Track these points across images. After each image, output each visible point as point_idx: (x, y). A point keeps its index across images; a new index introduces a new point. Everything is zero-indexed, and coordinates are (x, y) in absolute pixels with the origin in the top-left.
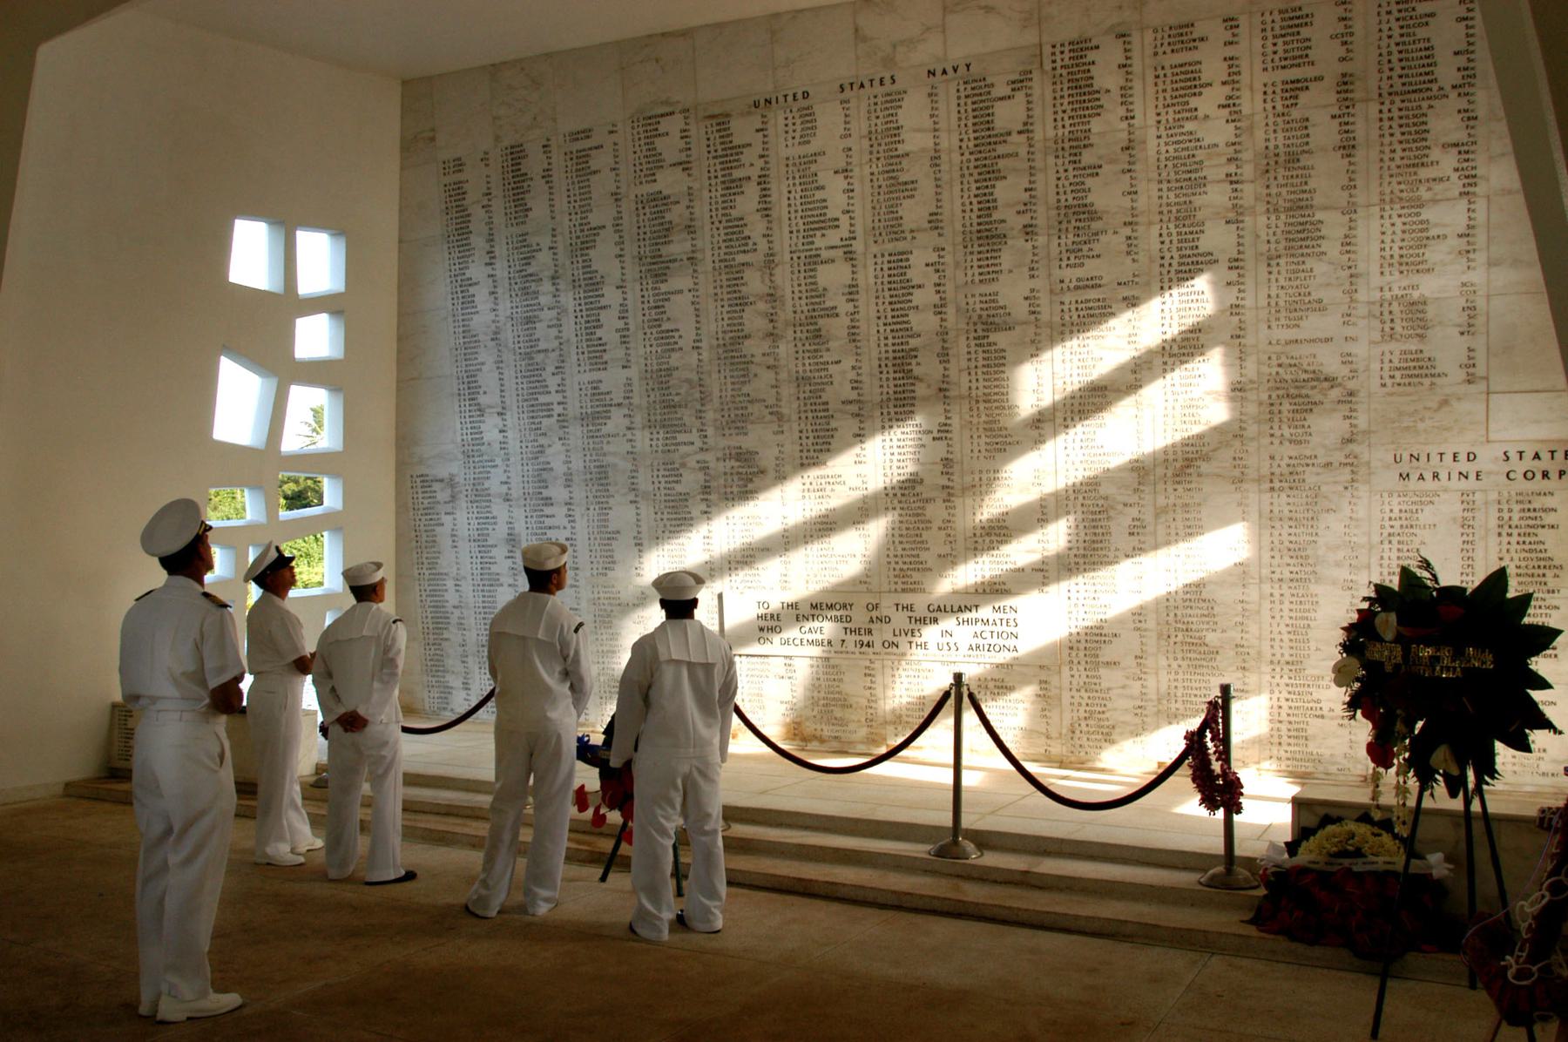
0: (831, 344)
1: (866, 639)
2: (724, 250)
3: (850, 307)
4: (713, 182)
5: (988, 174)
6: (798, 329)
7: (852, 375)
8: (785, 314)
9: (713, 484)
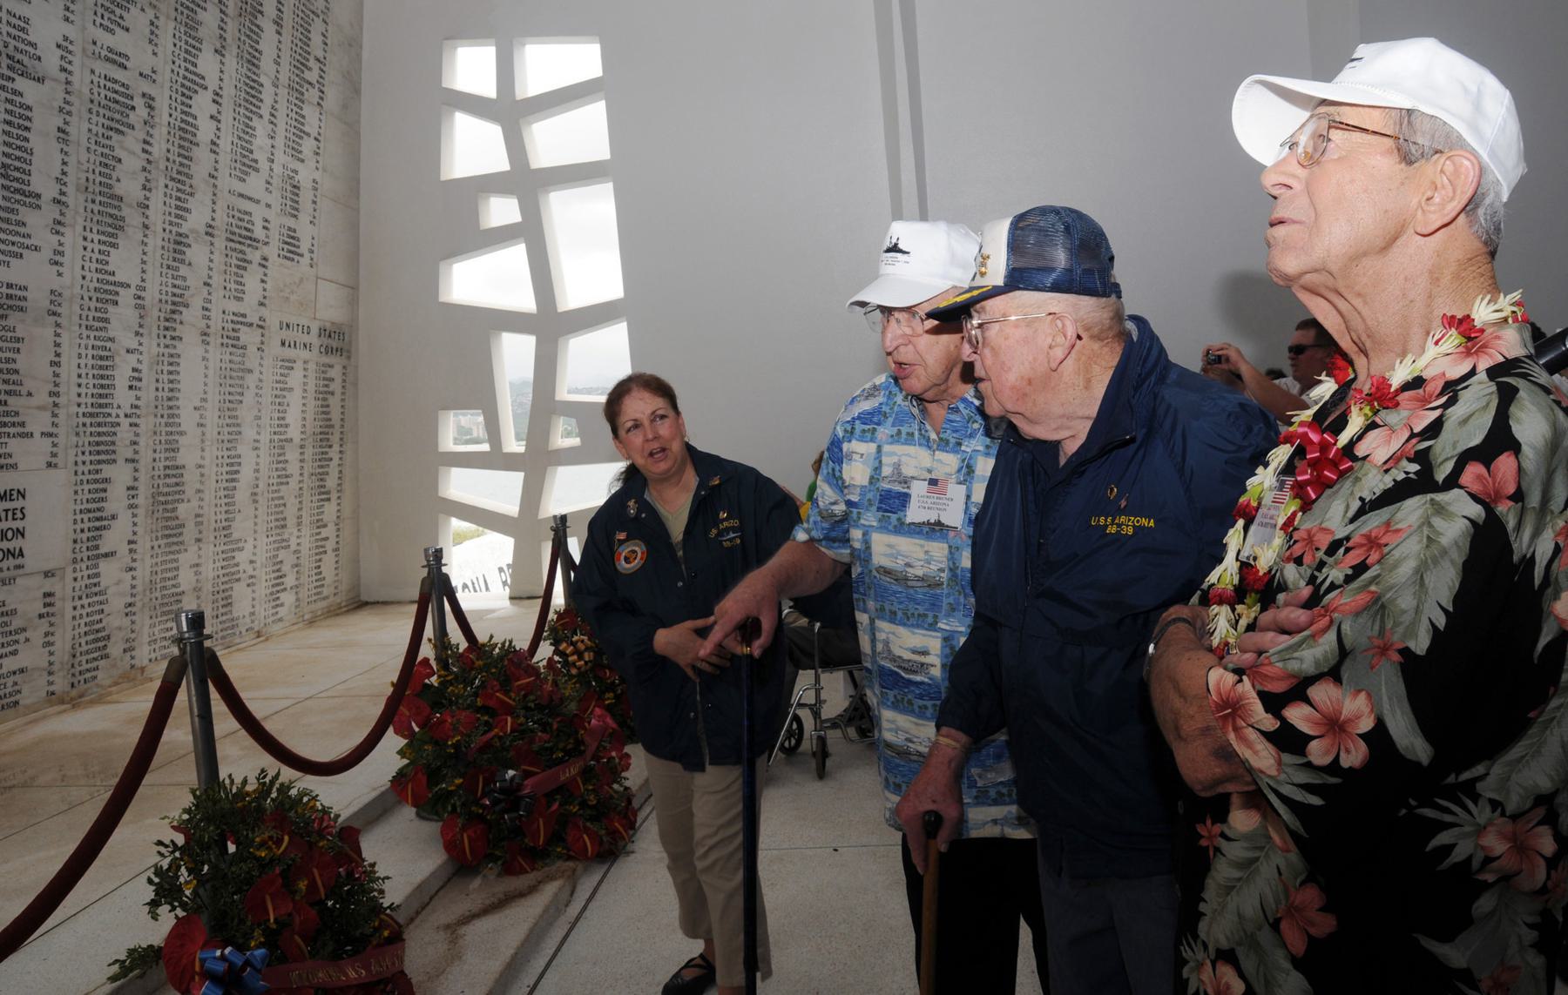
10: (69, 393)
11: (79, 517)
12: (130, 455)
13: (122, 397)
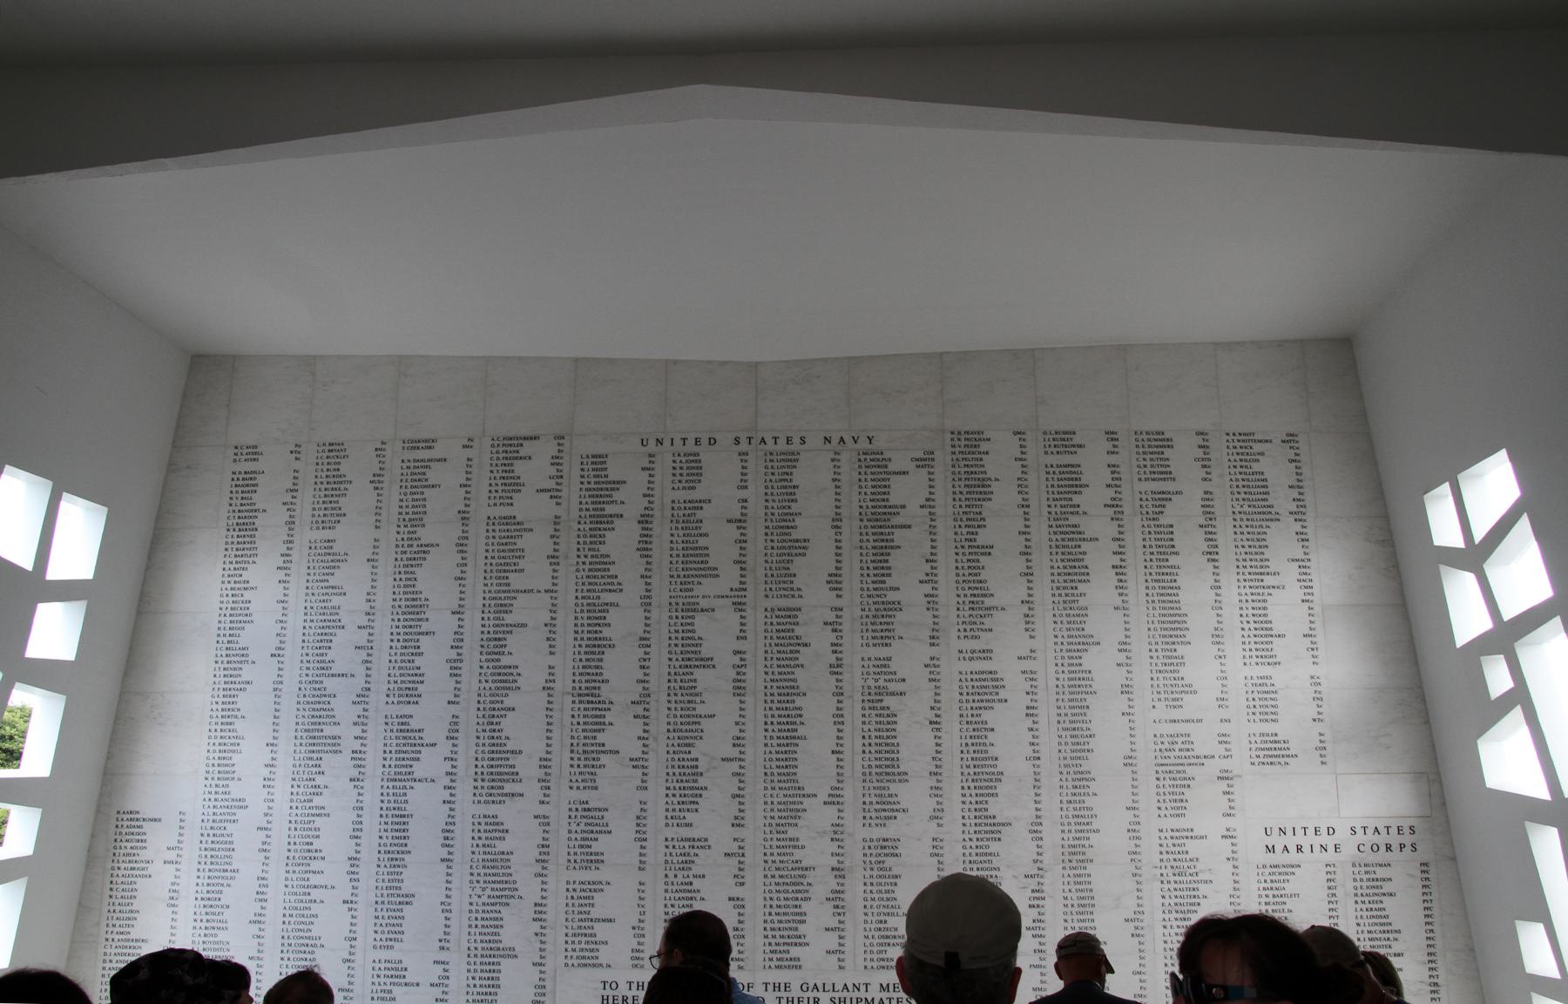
0: (704, 697)
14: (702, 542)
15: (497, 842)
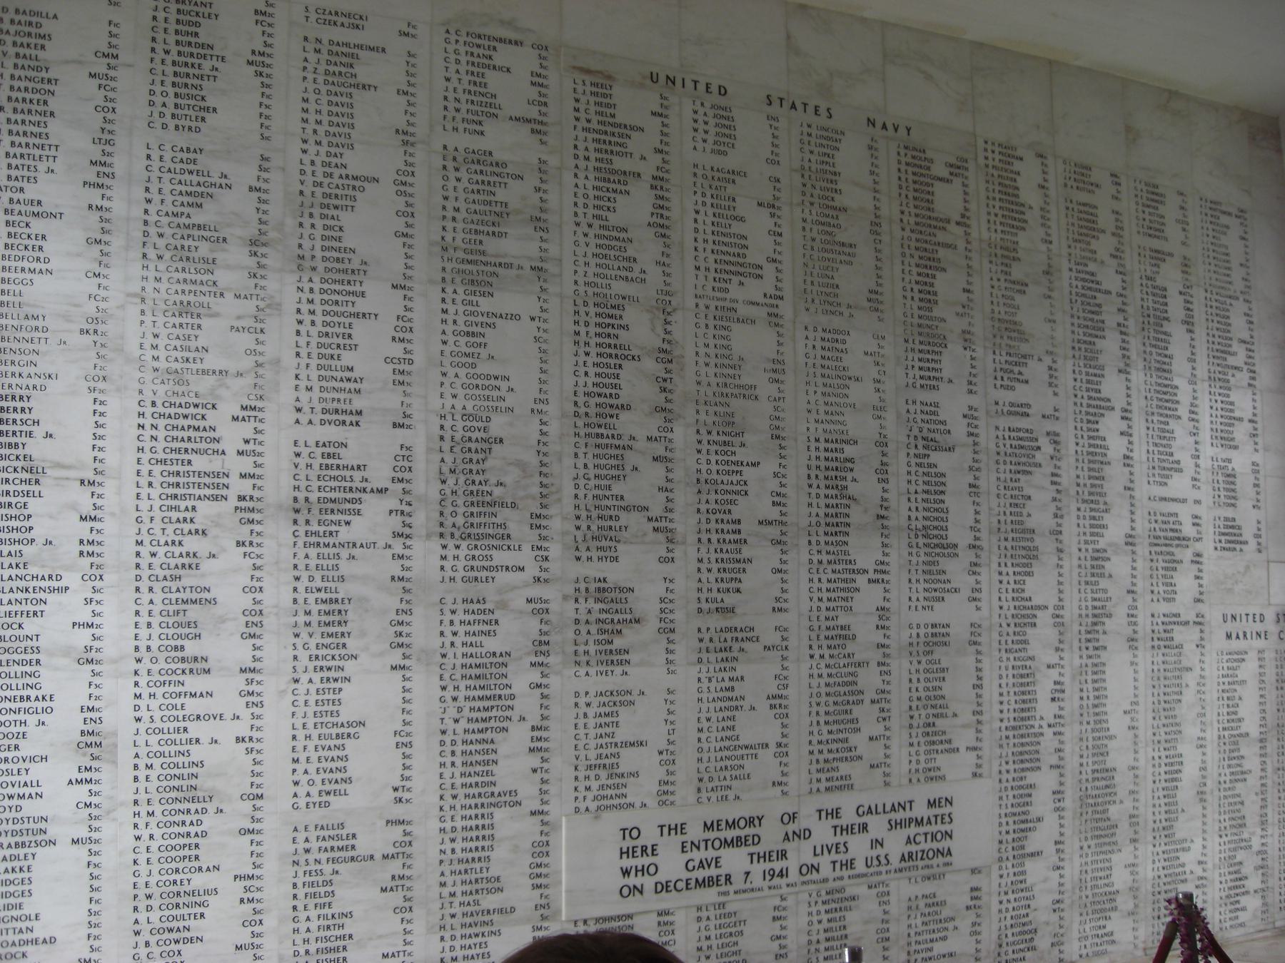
0: (748, 438)
1: (777, 865)
2: (592, 270)
3: (772, 389)
4: (582, 164)
5: (929, 264)
6: (702, 408)
7: (773, 485)
8: (684, 384)
9: (553, 638)
10: (992, 710)
11: (1004, 820)
12: (1054, 760)
13: (1045, 709)
14: (737, 228)
15: (483, 638)
